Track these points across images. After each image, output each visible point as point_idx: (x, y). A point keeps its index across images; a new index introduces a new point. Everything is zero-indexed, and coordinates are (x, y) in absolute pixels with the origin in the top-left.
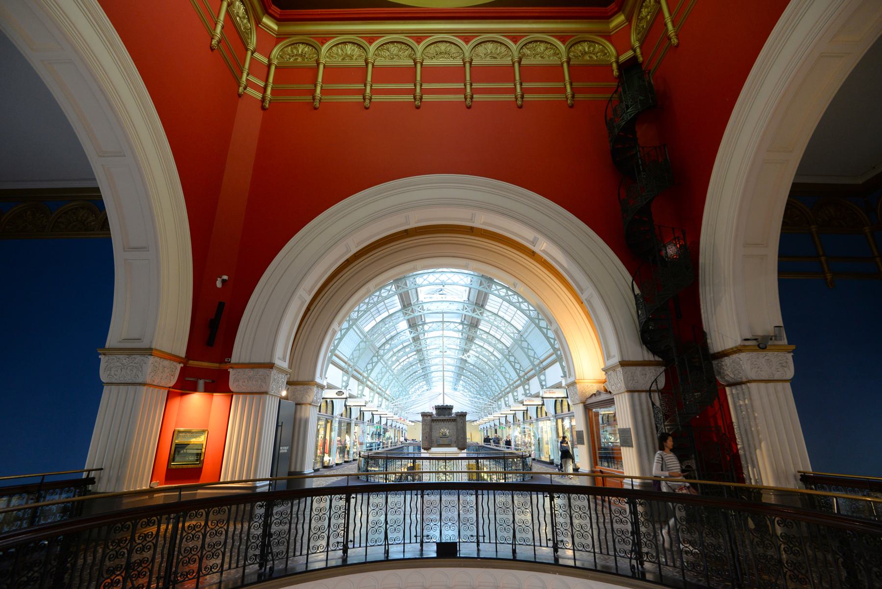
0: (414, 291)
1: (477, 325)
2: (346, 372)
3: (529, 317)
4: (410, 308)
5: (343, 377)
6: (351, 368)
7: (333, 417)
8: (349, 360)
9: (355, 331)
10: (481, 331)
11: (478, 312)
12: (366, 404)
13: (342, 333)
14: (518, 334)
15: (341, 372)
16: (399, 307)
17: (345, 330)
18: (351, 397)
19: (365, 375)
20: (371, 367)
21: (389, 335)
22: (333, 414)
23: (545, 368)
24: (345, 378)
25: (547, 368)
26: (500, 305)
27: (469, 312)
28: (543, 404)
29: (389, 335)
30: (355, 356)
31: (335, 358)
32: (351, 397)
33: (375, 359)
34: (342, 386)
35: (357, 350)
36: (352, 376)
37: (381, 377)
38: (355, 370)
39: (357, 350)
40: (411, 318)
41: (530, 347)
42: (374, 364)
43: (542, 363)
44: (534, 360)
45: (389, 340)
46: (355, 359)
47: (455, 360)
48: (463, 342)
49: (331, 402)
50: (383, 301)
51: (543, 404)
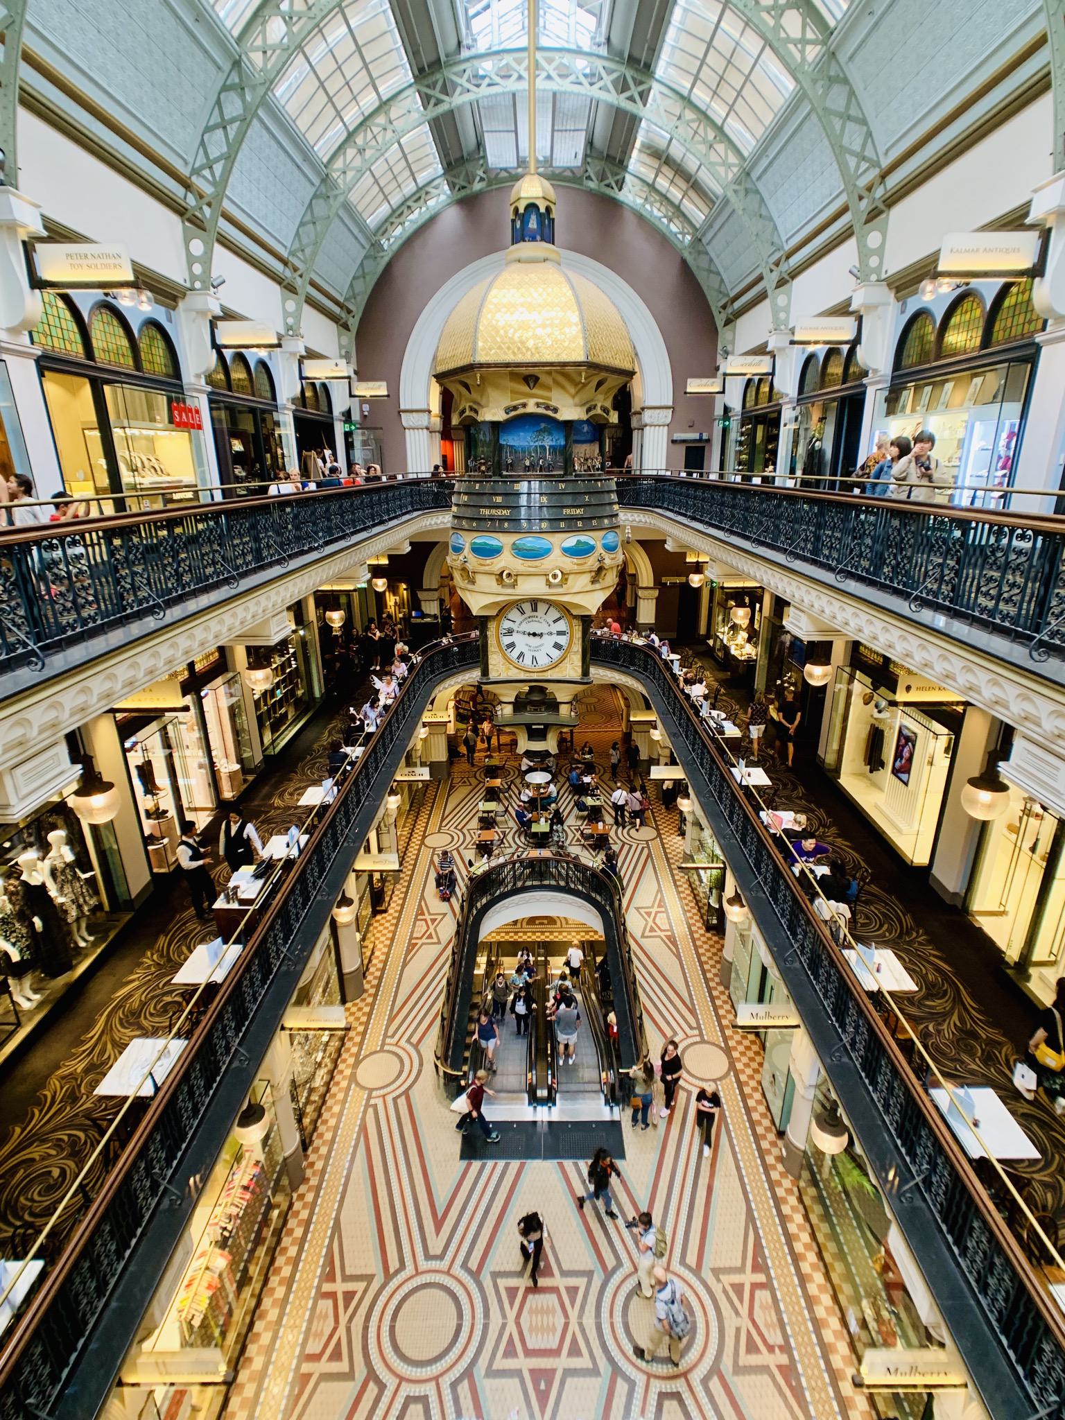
1: (621, 162)
2: (290, 288)
4: (438, 76)
5: (284, 301)
6: (301, 276)
7: (181, 387)
8: (292, 253)
9: (267, 129)
11: (634, 91)
12: (279, 339)
13: (231, 137)
14: (824, 43)
15: (277, 287)
16: (405, 75)
17: (237, 124)
18: (311, 355)
19: (208, 190)
22: (274, 398)
23: (794, 274)
24: (197, 247)
27: (609, 91)
28: (1037, 271)
30: (214, 153)
32: (311, 355)
34: (193, 278)
35: (216, 127)
36: (219, 241)
38: (28, 58)
39: (216, 127)
40: (444, 115)
44: (858, 167)
46: (308, 251)
51: (1037, 271)
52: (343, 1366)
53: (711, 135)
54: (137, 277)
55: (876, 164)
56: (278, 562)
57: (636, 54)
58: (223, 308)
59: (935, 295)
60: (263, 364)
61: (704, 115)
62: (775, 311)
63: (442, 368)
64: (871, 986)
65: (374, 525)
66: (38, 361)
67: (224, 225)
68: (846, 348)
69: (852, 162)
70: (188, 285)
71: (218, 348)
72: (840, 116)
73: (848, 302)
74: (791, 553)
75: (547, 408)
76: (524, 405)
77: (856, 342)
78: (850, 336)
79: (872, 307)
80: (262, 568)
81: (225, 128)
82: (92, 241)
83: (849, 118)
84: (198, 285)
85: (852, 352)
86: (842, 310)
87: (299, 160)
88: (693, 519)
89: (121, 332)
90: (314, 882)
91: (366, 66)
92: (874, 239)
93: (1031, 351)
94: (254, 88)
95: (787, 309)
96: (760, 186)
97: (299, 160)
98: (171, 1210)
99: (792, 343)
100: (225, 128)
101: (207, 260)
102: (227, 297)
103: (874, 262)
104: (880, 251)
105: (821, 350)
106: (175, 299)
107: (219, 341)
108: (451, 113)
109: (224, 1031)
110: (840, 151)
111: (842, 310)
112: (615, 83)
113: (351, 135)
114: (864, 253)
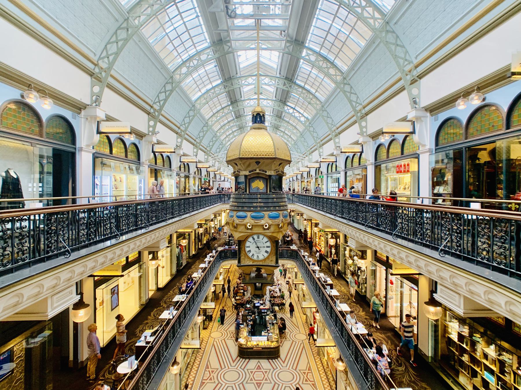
0: (238, 89)
3: (335, 82)
5: (177, 139)
10: (288, 107)
13: (167, 95)
14: (341, 76)
15: (175, 135)
18: (184, 155)
20: (188, 121)
21: (216, 109)
25: (342, 133)
26: (306, 76)
29: (216, 109)
31: (161, 117)
32: (184, 155)
33: (205, 129)
34: (149, 131)
37: (203, 135)
39: (163, 92)
41: (399, 43)
42: (204, 132)
43: (338, 129)
44: (356, 105)
45: (186, 61)
47: (273, 102)
48: (282, 82)
49: (160, 156)
50: (217, 97)
52: (213, 381)
53: (311, 97)
54: (131, 131)
55: (361, 104)
56: (178, 216)
57: (282, 99)
58: (183, 153)
59: (385, 140)
60: (168, 157)
61: (309, 91)
62: (335, 143)
63: (228, 159)
64: (355, 332)
65: (211, 205)
66: (93, 154)
67: (186, 136)
68: (359, 154)
69: (330, 125)
70: (147, 133)
71: (154, 152)
72: (349, 92)
73: (358, 141)
74: (348, 219)
75: (263, 171)
76: (256, 170)
77: (361, 153)
78: (361, 150)
79: (365, 143)
80: (158, 223)
81: (165, 93)
82: (166, 144)
83: (351, 93)
84: (150, 134)
85: (361, 155)
86: (357, 143)
87: (202, 119)
88: (304, 205)
89: (123, 146)
90: (171, 340)
91: (220, 102)
92: (363, 124)
93: (366, 167)
94: (197, 110)
95: (339, 143)
96: (327, 109)
97: (202, 119)
98: (165, 362)
99: (341, 152)
100: (165, 93)
101: (154, 127)
102: (159, 137)
103: (364, 130)
104: (366, 127)
105: (351, 155)
106: (142, 137)
107: (155, 150)
108: (234, 90)
109: (143, 381)
110: (350, 101)
111: (357, 143)
112: (277, 105)
113: (214, 114)
114: (361, 127)
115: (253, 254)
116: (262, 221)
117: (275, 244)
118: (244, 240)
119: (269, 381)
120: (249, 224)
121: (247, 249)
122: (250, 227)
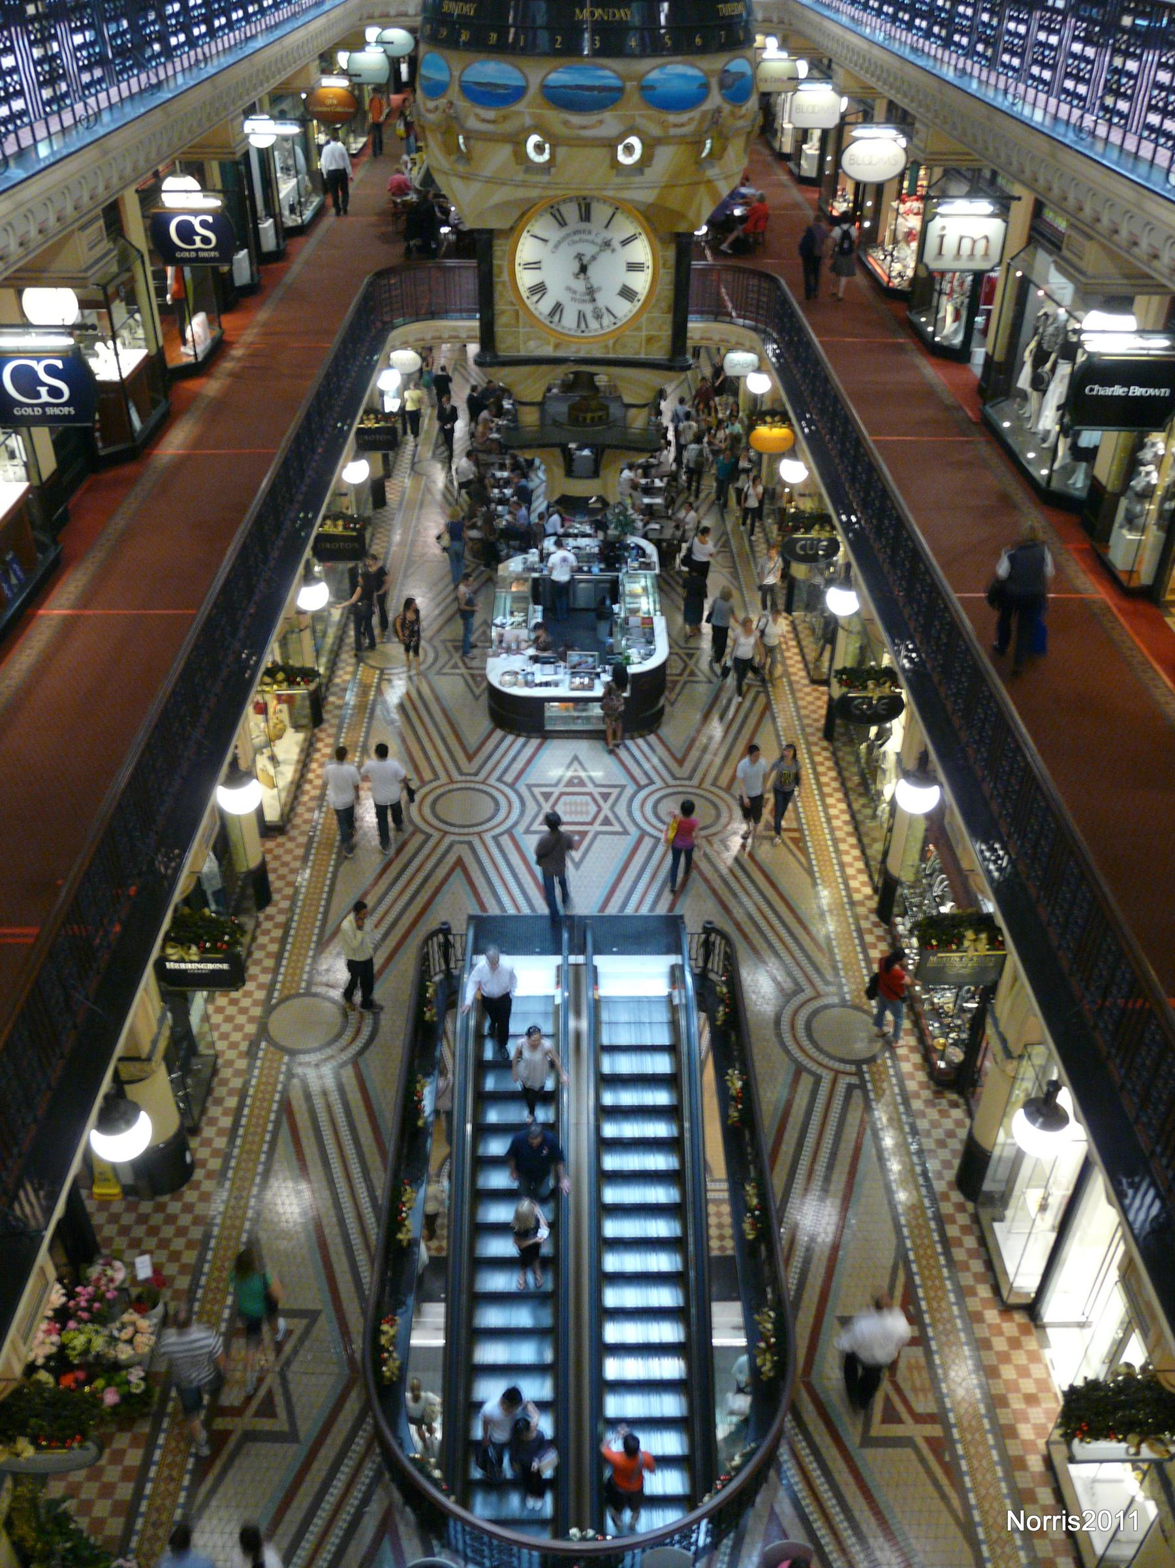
115: (558, 308)
116: (607, 115)
117: (671, 253)
118: (512, 229)
119: (618, 828)
120: (534, 139)
121: (526, 279)
122: (546, 156)
